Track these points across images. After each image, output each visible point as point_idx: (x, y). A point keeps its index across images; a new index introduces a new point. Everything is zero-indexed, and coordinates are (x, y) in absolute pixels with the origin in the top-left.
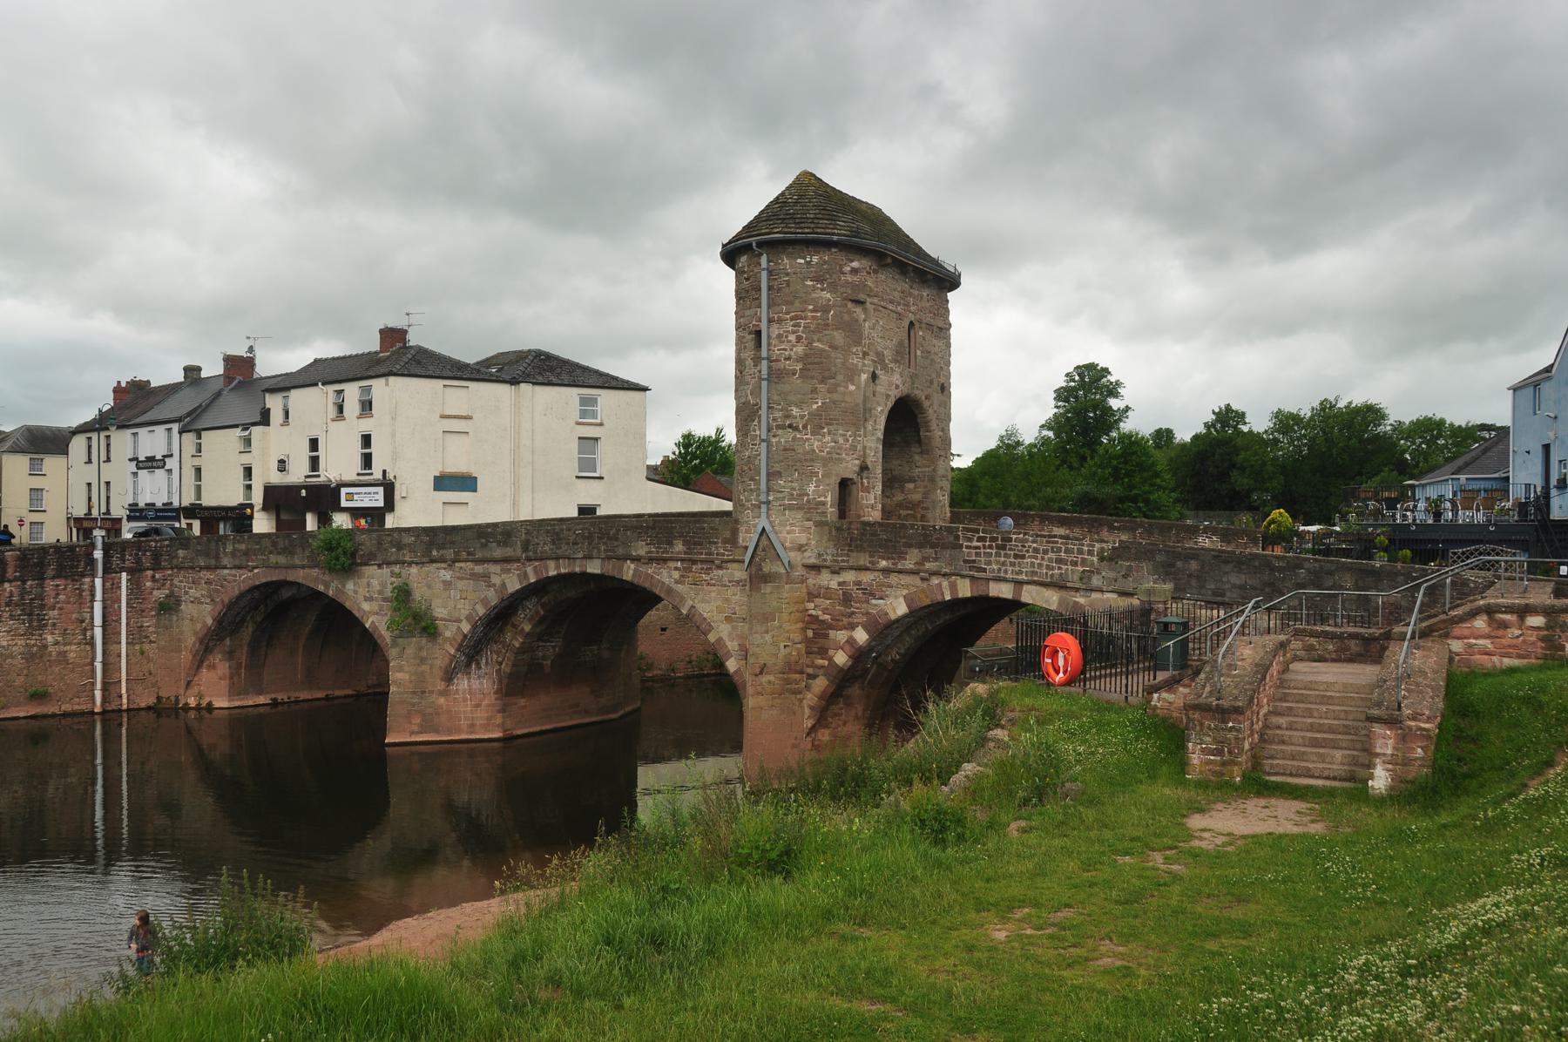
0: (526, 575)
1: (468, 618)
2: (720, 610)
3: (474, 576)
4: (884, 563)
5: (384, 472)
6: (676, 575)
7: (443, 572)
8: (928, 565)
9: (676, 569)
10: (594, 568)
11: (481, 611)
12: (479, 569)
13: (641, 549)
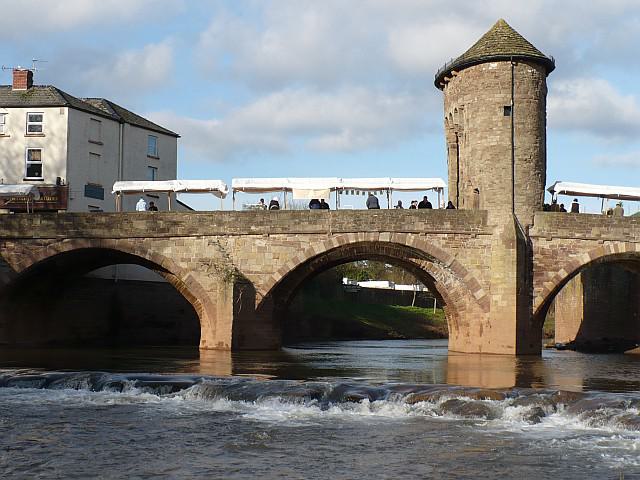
0: (330, 242)
1: (279, 271)
2: (473, 262)
3: (286, 243)
4: (577, 235)
5: (59, 179)
6: (444, 242)
7: (257, 242)
8: (603, 236)
9: (444, 239)
10: (384, 237)
11: (292, 266)
12: (290, 239)
13: (421, 226)
